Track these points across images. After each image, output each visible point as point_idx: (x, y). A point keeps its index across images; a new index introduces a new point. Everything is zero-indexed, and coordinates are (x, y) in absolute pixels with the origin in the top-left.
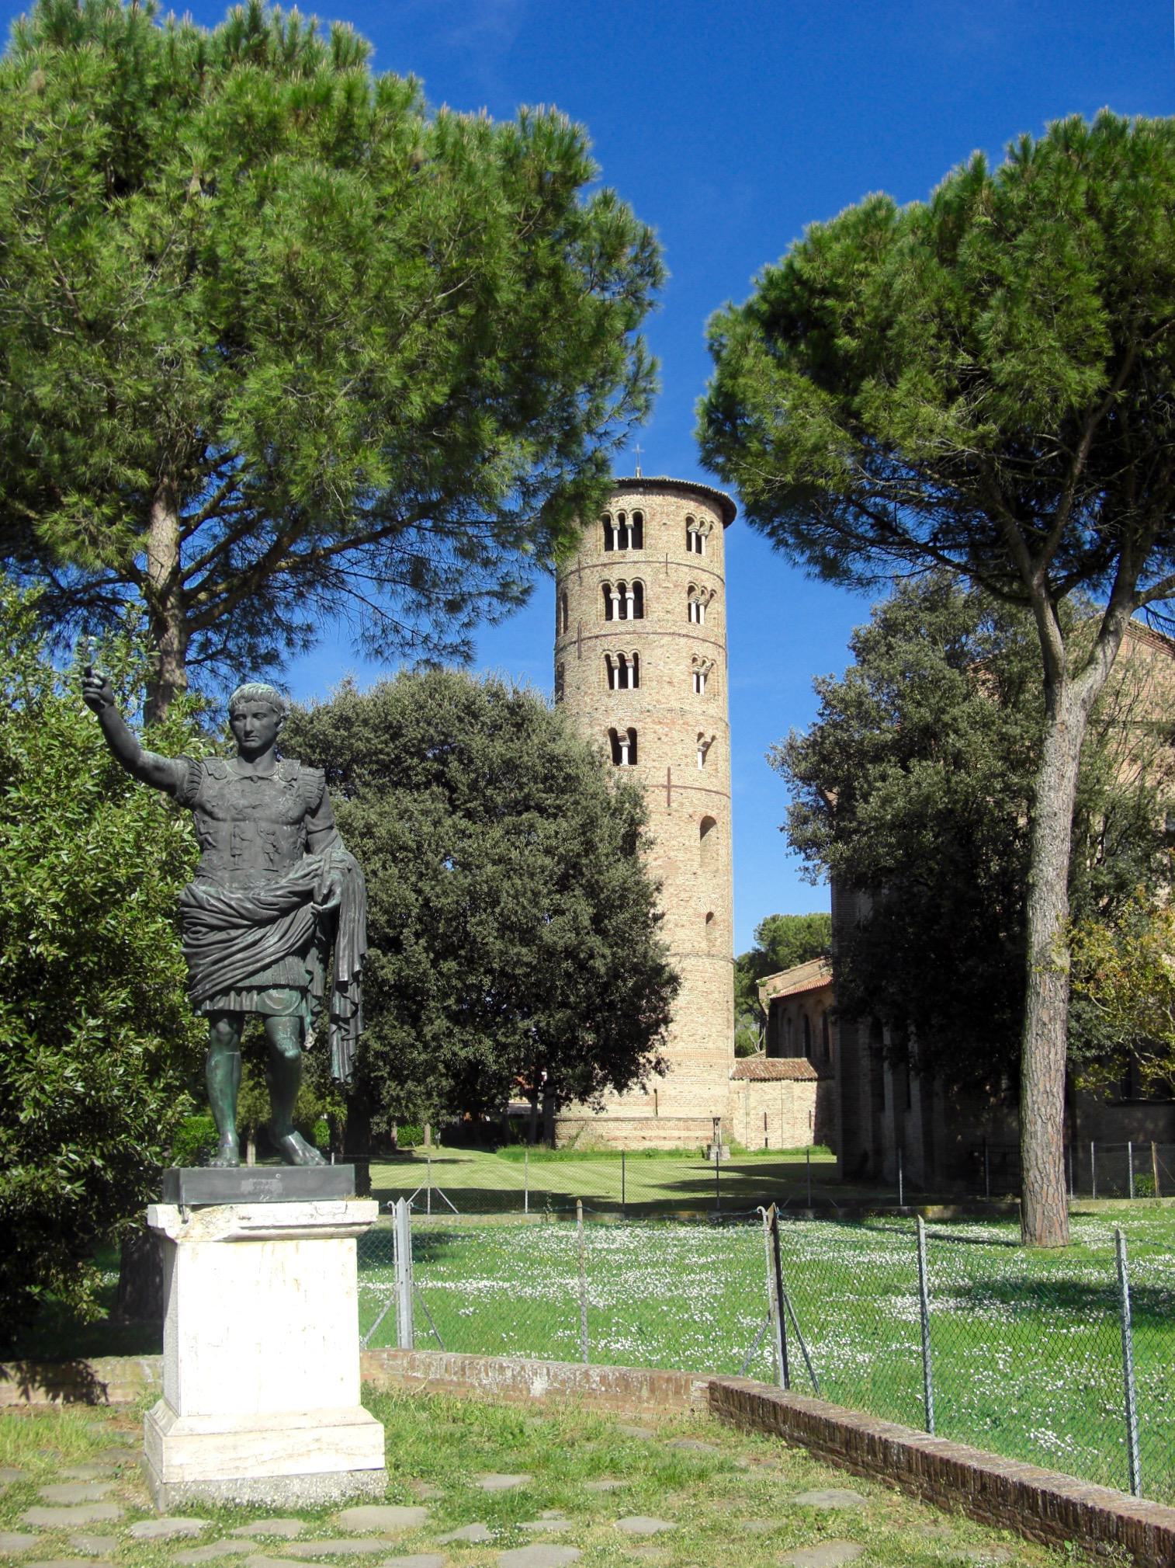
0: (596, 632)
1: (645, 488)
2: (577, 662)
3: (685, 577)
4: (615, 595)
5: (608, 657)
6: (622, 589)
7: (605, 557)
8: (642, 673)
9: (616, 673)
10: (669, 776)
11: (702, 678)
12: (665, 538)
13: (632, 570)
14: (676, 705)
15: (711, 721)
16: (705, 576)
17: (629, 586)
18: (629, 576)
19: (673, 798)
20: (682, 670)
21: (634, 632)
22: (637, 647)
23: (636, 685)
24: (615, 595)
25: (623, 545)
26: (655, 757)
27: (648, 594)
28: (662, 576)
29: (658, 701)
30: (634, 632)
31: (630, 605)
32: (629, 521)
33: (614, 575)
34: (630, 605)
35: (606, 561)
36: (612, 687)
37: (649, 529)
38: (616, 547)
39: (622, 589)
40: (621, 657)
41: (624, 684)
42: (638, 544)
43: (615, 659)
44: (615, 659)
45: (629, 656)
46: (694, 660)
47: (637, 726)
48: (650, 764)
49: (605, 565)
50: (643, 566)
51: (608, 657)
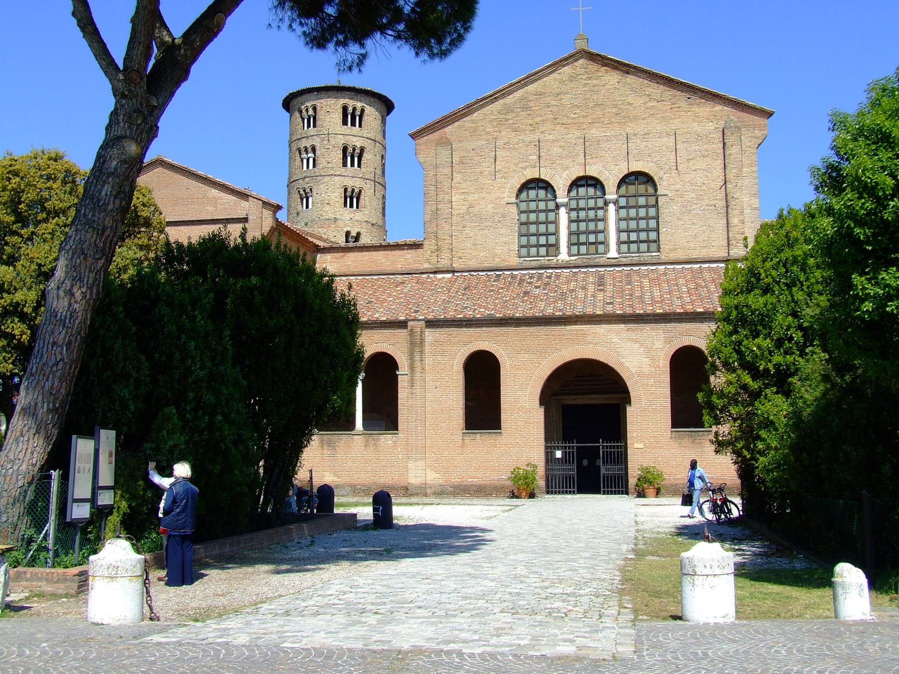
3: (341, 141)
11: (355, 200)
14: (332, 216)
15: (356, 223)
16: (355, 139)
17: (309, 150)
20: (337, 196)
29: (322, 215)
31: (311, 161)
32: (311, 112)
34: (311, 161)
37: (321, 115)
41: (307, 207)
42: (315, 126)
45: (308, 190)
46: (346, 190)
49: (299, 139)
50: (315, 137)
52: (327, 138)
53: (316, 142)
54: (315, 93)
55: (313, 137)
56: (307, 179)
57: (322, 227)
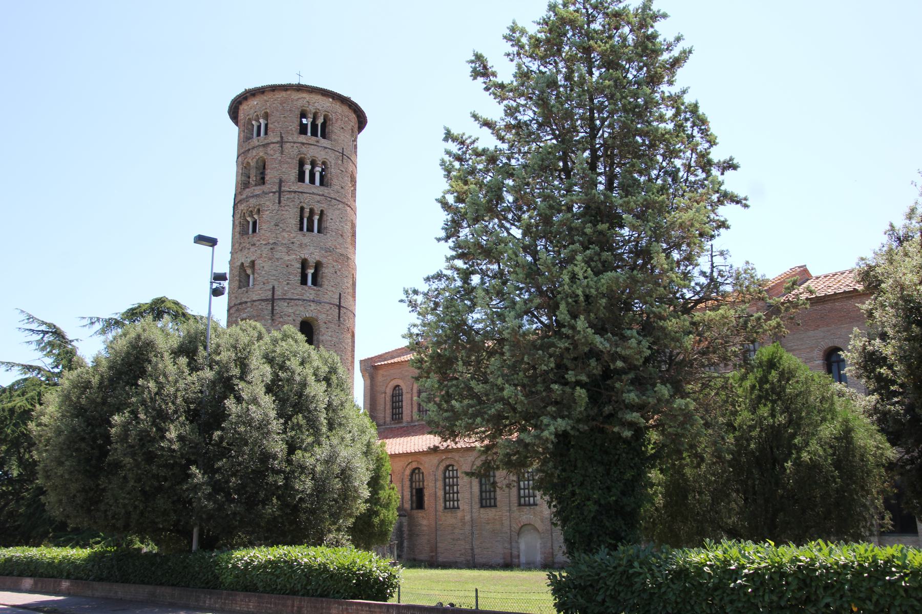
0: (294, 188)
1: (333, 98)
2: (276, 206)
4: (308, 168)
5: (302, 209)
6: (313, 164)
7: (302, 138)
8: (324, 225)
9: (305, 220)
10: (340, 298)
12: (342, 137)
13: (323, 153)
18: (320, 155)
19: (341, 315)
21: (323, 195)
22: (324, 206)
23: (319, 231)
24: (308, 168)
25: (314, 133)
26: (332, 284)
27: (333, 170)
28: (340, 162)
30: (323, 195)
33: (311, 152)
35: (305, 141)
36: (301, 229)
38: (309, 134)
39: (313, 164)
40: (312, 212)
43: (307, 210)
44: (307, 210)
45: (317, 211)
47: (324, 261)
48: (330, 288)
49: (303, 144)
51: (302, 209)
52: (341, 158)
53: (331, 158)
54: (331, 100)
55: (327, 150)
56: (318, 198)
57: (337, 262)
